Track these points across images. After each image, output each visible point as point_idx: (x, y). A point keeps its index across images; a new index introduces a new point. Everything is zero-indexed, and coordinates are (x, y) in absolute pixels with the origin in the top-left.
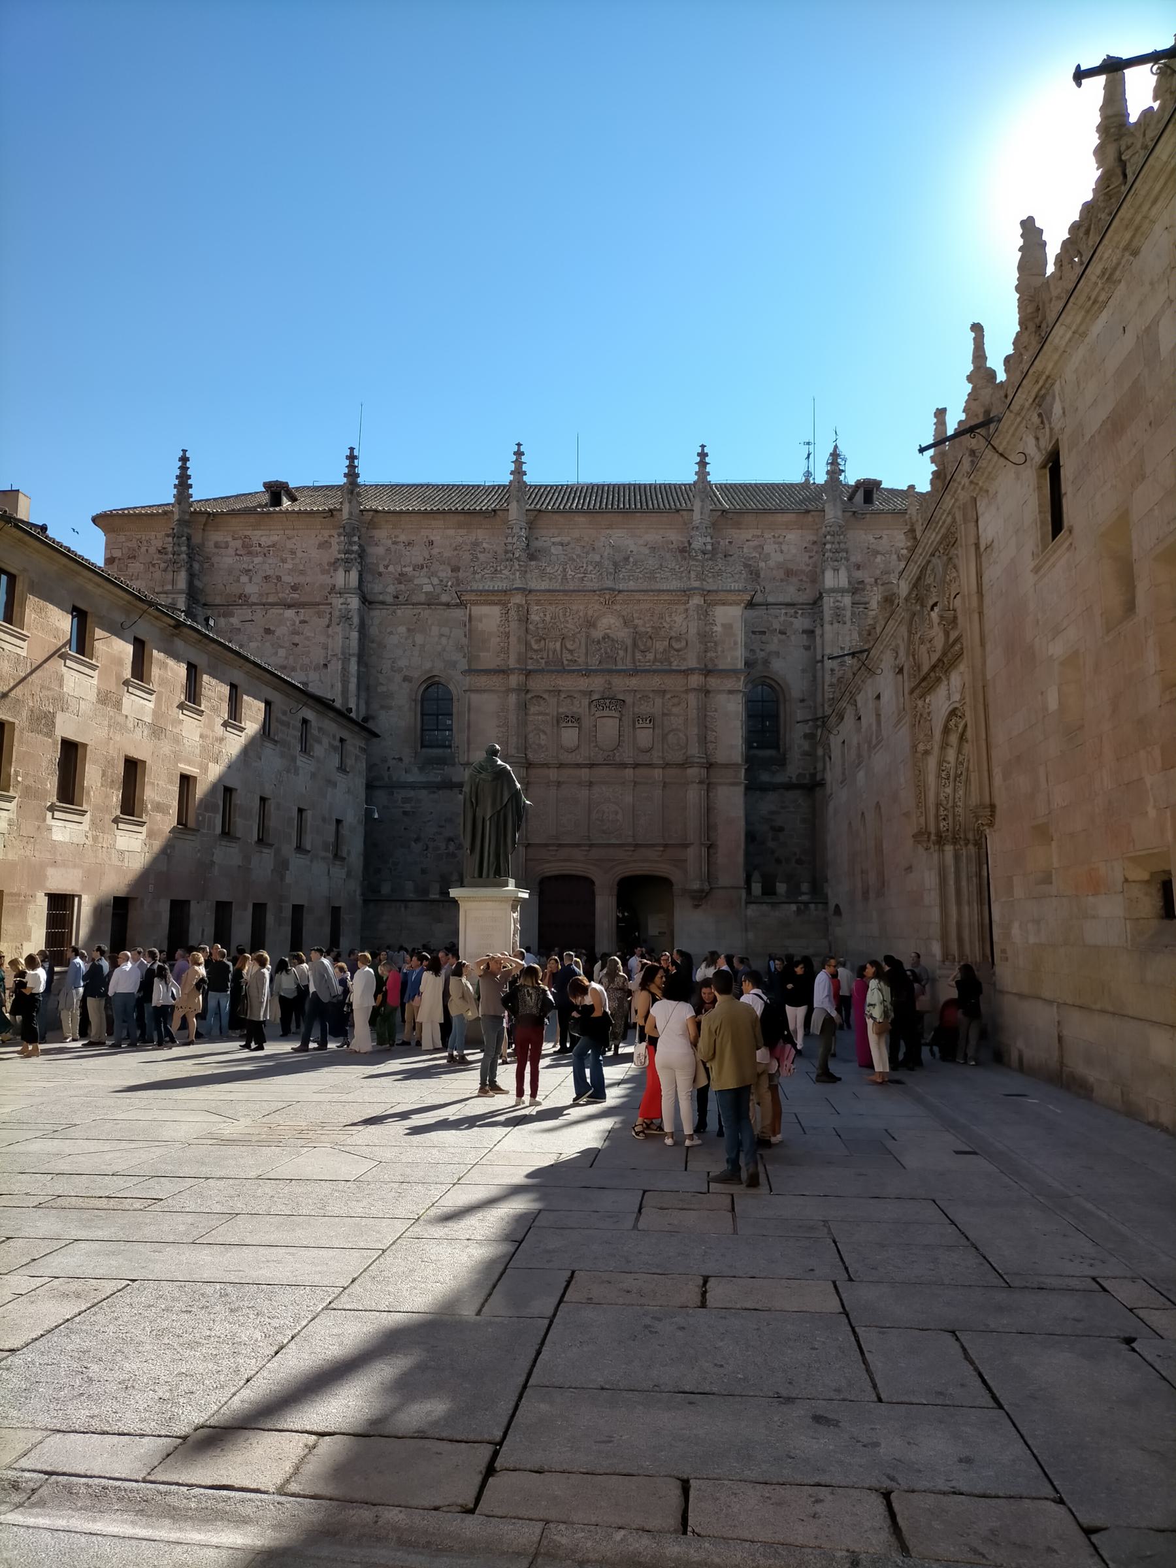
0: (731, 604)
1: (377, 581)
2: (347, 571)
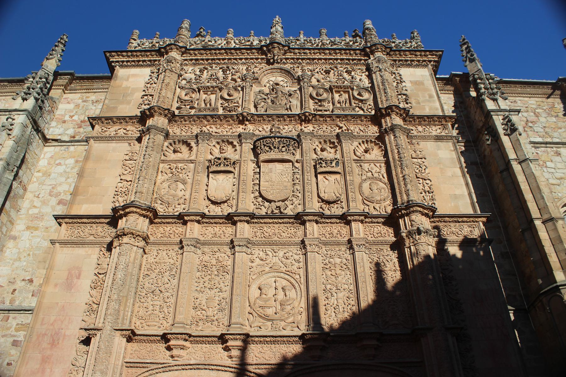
0: (417, 66)
1: (59, 126)
2: (24, 99)
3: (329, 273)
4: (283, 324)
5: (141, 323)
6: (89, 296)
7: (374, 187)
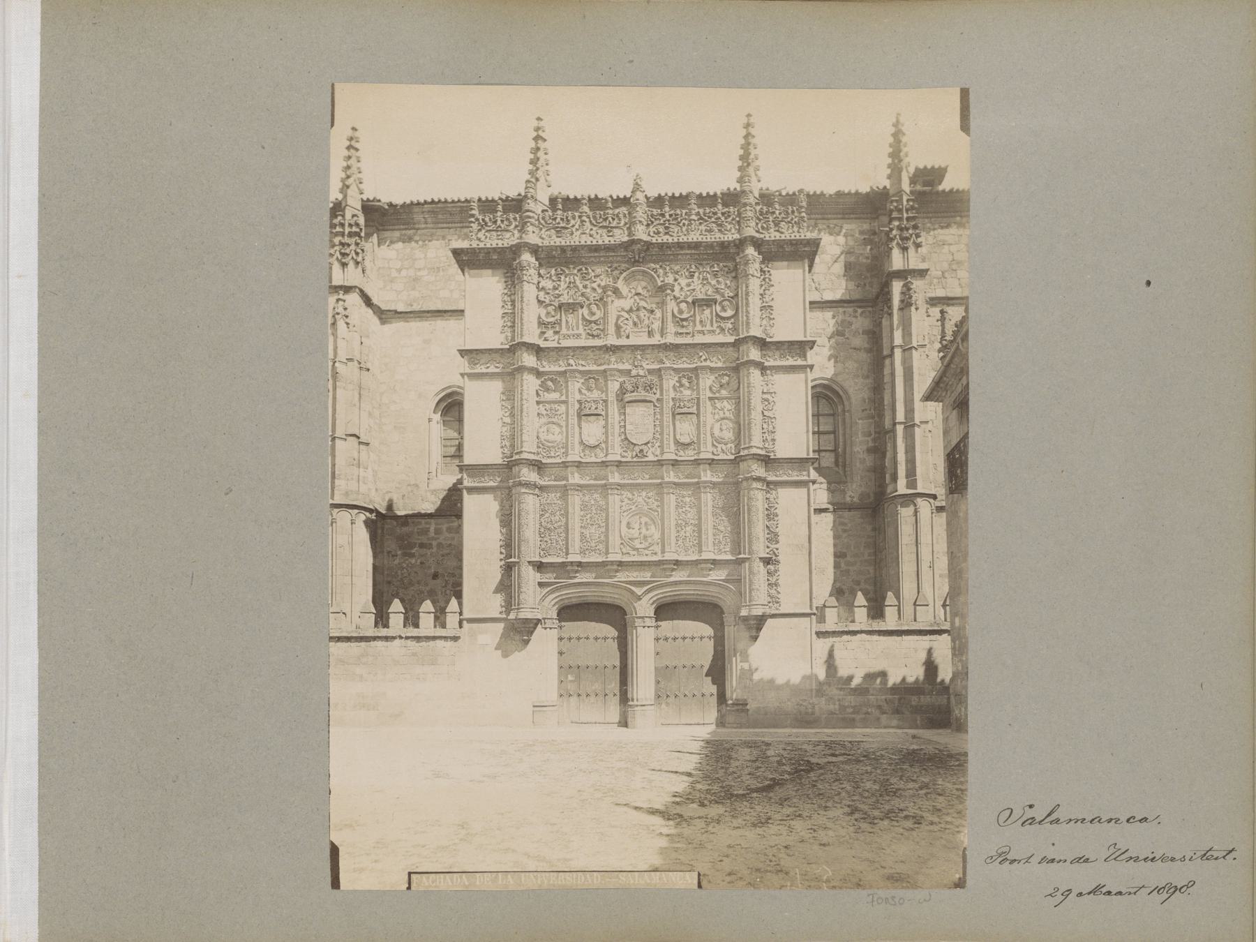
3: (680, 510)
4: (647, 552)
5: (545, 554)
6: (500, 534)
7: (724, 427)
